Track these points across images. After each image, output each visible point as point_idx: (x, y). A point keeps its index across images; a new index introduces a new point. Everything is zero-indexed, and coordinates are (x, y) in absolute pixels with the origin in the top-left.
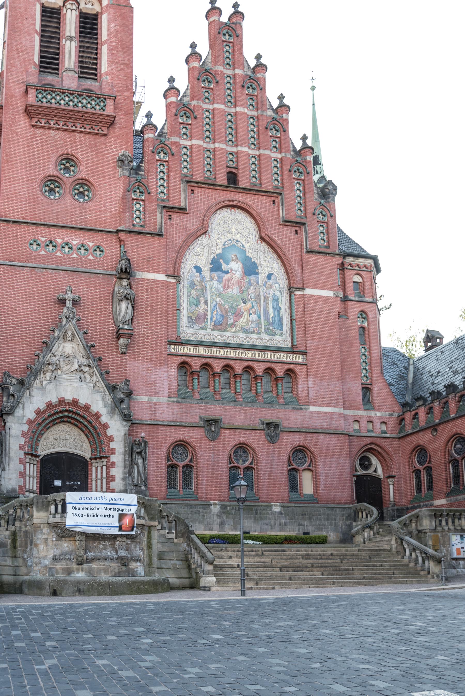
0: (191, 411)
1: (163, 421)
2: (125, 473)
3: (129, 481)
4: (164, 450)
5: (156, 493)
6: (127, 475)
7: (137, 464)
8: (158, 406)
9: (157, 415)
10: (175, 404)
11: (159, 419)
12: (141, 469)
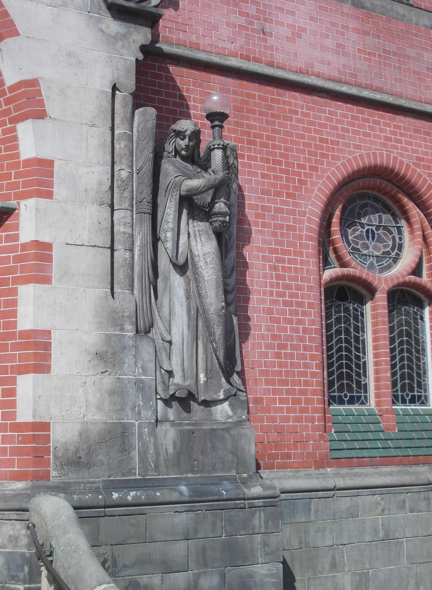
0: (411, 52)
1: (300, 71)
3: (139, 366)
4: (312, 207)
5: (280, 431)
6: (129, 331)
9: (271, 41)
11: (280, 58)
12: (213, 299)
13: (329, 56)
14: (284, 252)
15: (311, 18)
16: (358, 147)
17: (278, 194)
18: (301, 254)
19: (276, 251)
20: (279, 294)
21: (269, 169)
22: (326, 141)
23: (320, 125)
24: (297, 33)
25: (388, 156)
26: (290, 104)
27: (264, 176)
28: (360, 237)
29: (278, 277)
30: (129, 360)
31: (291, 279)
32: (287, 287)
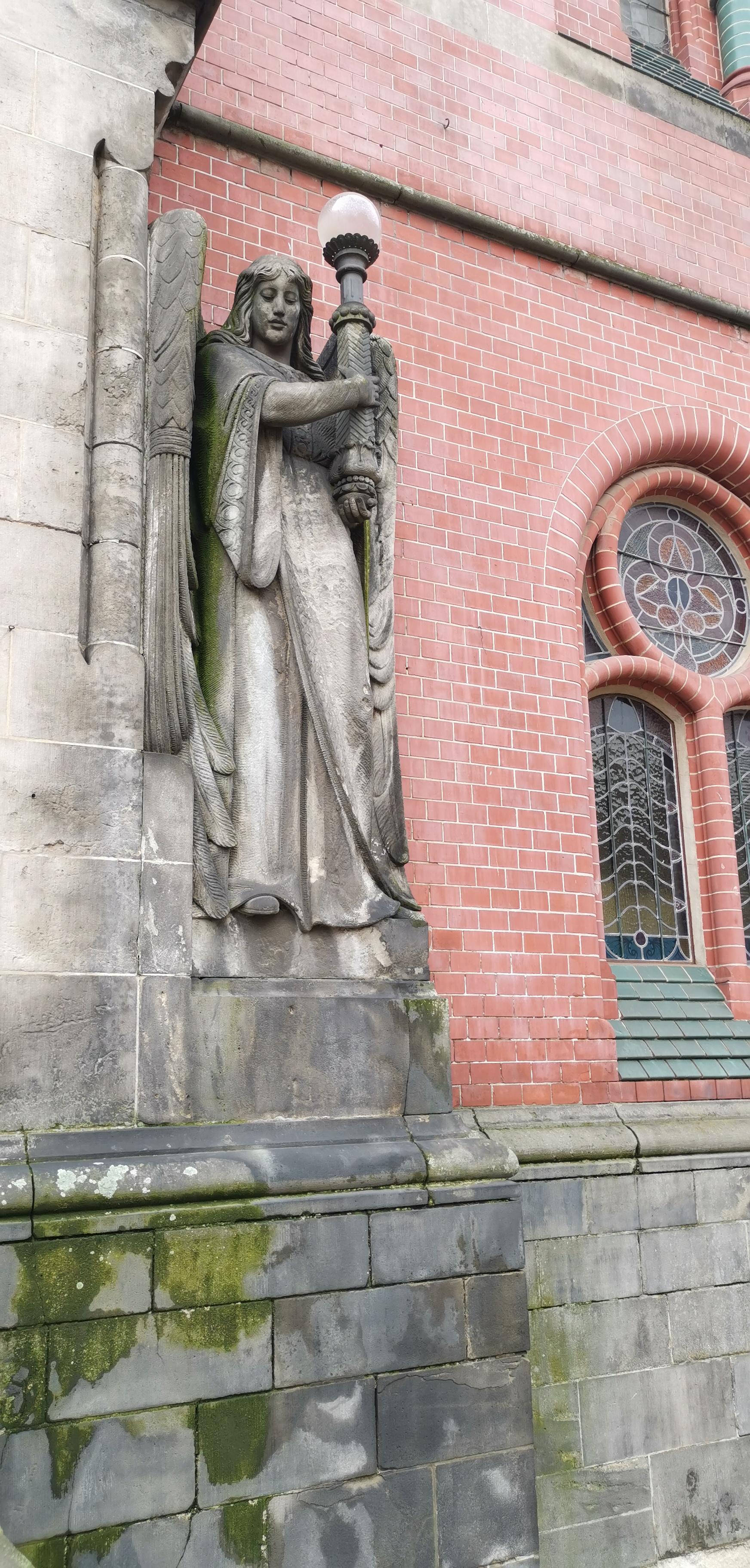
2: (84, 710)
3: (152, 832)
4: (558, 512)
5: (503, 1015)
6: (127, 741)
7: (272, 591)
8: (472, 72)
9: (466, 155)
10: (620, 107)
13: (588, 204)
14: (500, 605)
15: (549, 118)
16: (654, 393)
17: (487, 477)
18: (539, 612)
19: (484, 602)
20: (491, 698)
21: (465, 420)
22: (588, 374)
23: (573, 338)
24: (518, 147)
25: (716, 420)
26: (509, 285)
27: (453, 435)
28: (658, 596)
29: (489, 660)
30: (121, 815)
31: (519, 665)
32: (511, 683)
